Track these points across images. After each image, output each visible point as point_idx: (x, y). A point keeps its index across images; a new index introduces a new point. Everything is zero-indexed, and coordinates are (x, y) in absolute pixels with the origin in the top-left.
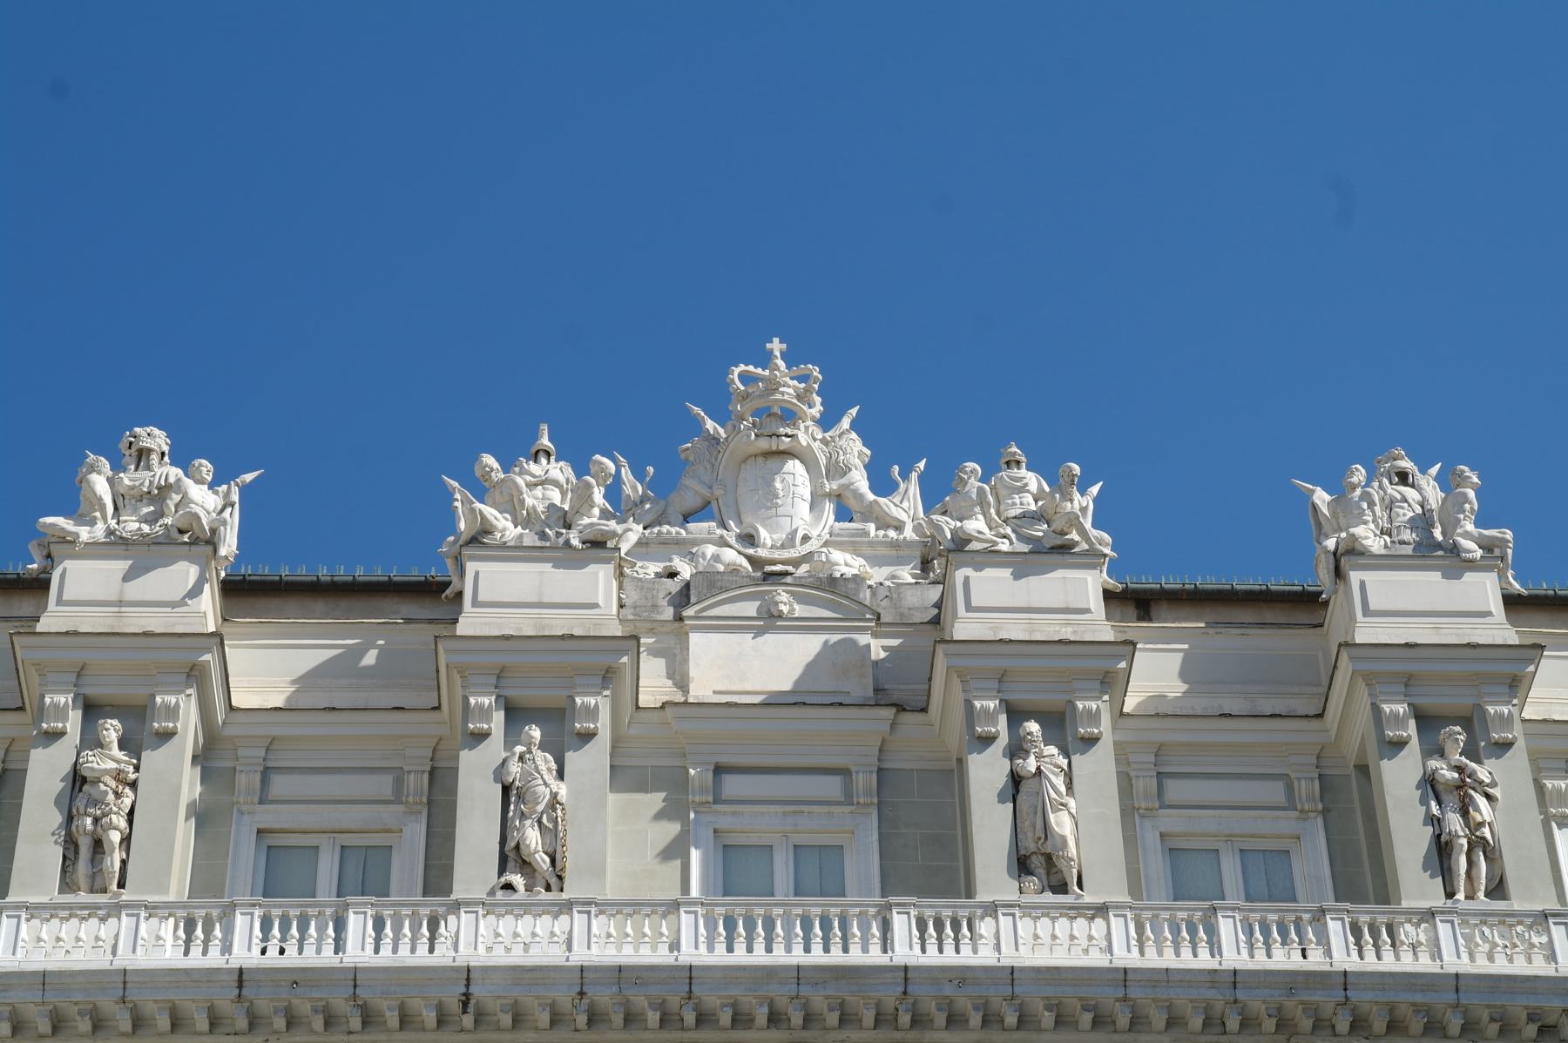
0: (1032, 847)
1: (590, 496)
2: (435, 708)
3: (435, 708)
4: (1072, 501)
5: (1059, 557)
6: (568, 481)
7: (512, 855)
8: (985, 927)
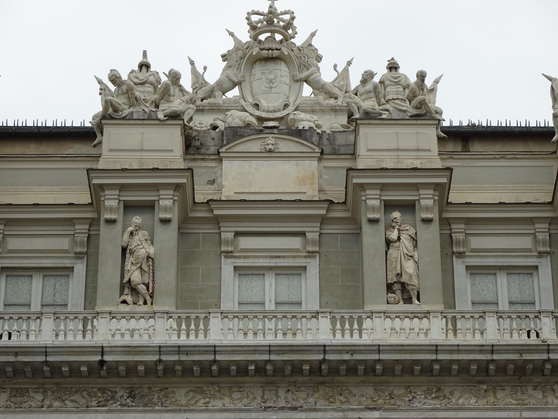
2: (89, 204)
8: (367, 324)
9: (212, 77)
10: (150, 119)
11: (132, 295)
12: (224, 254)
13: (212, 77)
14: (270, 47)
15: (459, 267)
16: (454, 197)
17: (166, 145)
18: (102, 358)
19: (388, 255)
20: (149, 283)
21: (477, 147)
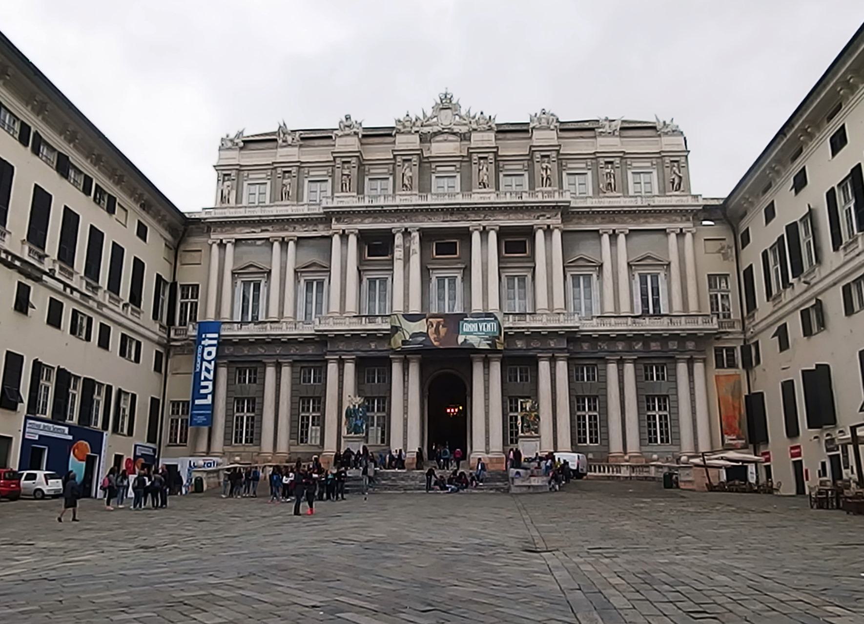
9: (429, 114)
10: (410, 132)
13: (429, 114)
14: (446, 104)
15: (501, 175)
16: (500, 153)
17: (413, 141)
21: (509, 135)
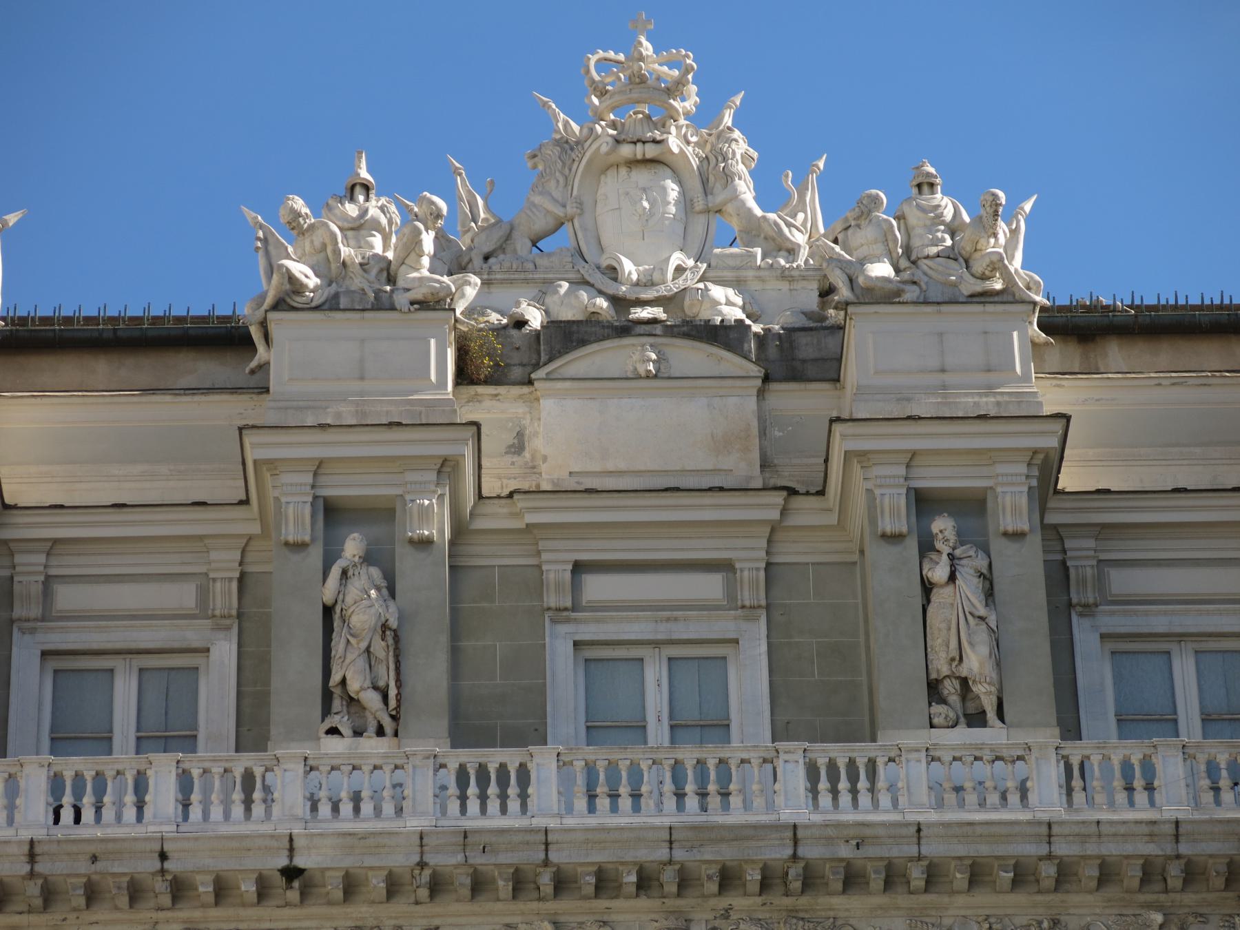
0: (945, 671)
1: (419, 243)
2: (241, 503)
3: (241, 503)
4: (995, 235)
5: (979, 308)
6: (390, 222)
7: (337, 691)
11: (349, 713)
12: (550, 613)
15: (1085, 635)
18: (291, 860)
19: (929, 614)
20: (388, 686)
